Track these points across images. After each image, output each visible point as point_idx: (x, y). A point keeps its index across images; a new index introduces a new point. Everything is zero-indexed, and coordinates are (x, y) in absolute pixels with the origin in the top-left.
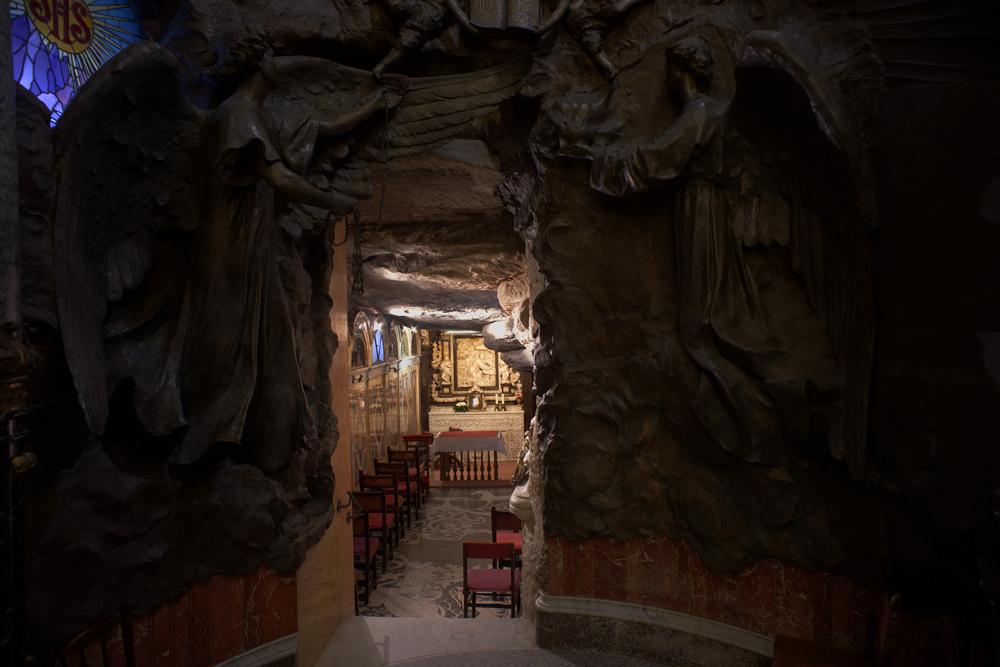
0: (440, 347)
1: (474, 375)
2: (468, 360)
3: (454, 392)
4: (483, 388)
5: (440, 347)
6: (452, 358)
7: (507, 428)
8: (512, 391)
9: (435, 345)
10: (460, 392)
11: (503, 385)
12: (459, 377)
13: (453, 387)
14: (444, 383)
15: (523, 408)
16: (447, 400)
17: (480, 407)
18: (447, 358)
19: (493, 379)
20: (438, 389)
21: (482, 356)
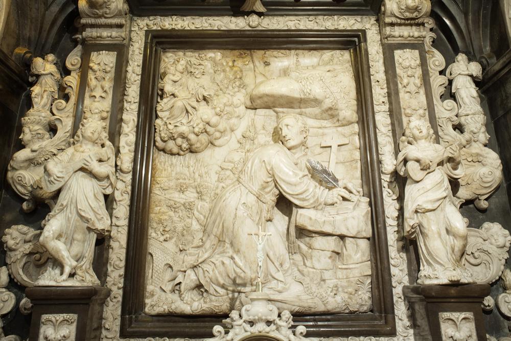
1: (246, 228)
2: (212, 158)
5: (73, 80)
6: (128, 138)
9: (45, 66)
13: (112, 312)
14: (50, 279)
21: (292, 132)
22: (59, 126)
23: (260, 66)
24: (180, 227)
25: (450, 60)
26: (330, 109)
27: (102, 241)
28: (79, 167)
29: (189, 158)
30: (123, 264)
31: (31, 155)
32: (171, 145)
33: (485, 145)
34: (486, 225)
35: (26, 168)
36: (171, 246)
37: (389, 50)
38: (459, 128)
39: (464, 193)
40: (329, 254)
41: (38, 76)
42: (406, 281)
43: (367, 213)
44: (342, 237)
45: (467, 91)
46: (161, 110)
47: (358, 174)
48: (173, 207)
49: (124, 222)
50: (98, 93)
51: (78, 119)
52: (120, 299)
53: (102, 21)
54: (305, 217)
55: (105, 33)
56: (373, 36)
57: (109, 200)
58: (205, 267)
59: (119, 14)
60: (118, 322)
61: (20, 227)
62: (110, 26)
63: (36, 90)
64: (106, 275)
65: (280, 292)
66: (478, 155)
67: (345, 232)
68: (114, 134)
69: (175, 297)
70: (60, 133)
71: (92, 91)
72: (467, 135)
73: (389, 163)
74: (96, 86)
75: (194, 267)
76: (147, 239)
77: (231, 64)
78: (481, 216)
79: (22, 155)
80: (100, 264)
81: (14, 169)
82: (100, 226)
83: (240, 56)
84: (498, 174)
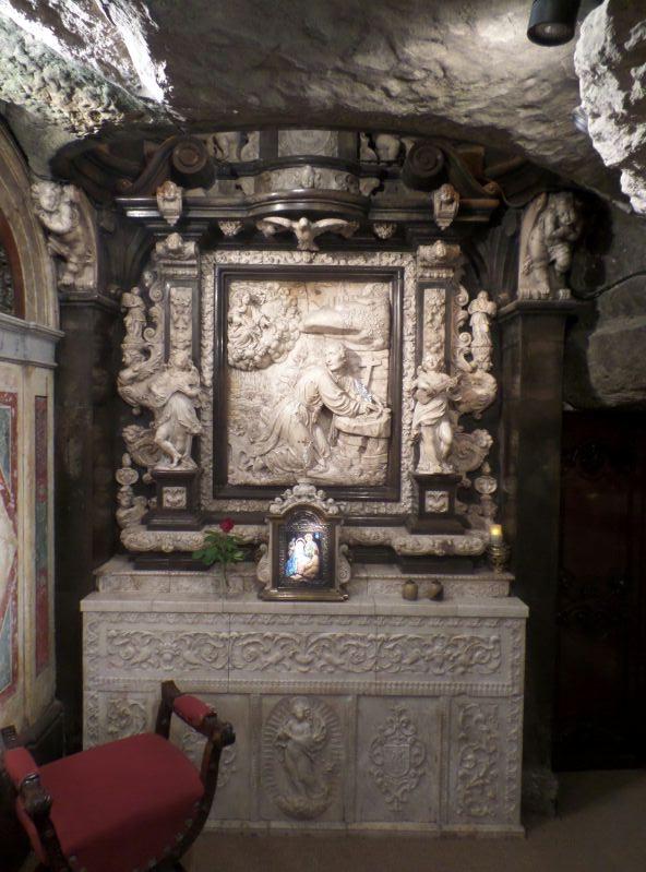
0: (157, 310)
3: (208, 503)
4: (335, 490)
6: (208, 359)
7: (445, 683)
8: (460, 507)
9: (133, 299)
10: (235, 506)
11: (424, 483)
12: (237, 443)
13: (207, 484)
14: (163, 466)
15: (516, 590)
16: (167, 540)
17: (322, 582)
18: (180, 356)
19: (376, 452)
20: (140, 488)
22: (152, 351)
23: (313, 296)
24: (250, 425)
25: (473, 296)
26: (366, 338)
27: (196, 440)
28: (175, 389)
29: (256, 374)
30: (211, 453)
31: (134, 374)
32: (241, 364)
33: (488, 372)
34: (478, 432)
35: (131, 384)
36: (244, 439)
37: (421, 287)
38: (469, 357)
39: (463, 408)
40: (357, 448)
41: (128, 309)
42: (410, 469)
43: (387, 422)
44: (367, 438)
45: (481, 326)
46: (232, 337)
47: (384, 389)
48: (246, 411)
49: (209, 424)
50: (181, 324)
51: (168, 345)
52: (211, 475)
53: (178, 262)
54: (342, 422)
55: (180, 271)
56: (409, 272)
57: (198, 411)
58: (269, 455)
59: (191, 258)
60: (211, 489)
61: (134, 427)
62: (185, 266)
63: (129, 320)
64: (200, 460)
65: (321, 472)
66: (479, 379)
67: (367, 433)
68: (196, 358)
69: (249, 474)
70: (153, 357)
71: (175, 322)
72: (473, 363)
73: (407, 384)
74: (178, 320)
75: (261, 456)
76: (227, 435)
77: (287, 292)
78: (475, 424)
79: (127, 374)
80: (195, 453)
81: (122, 385)
82: (195, 431)
83: (295, 286)
84: (492, 393)
